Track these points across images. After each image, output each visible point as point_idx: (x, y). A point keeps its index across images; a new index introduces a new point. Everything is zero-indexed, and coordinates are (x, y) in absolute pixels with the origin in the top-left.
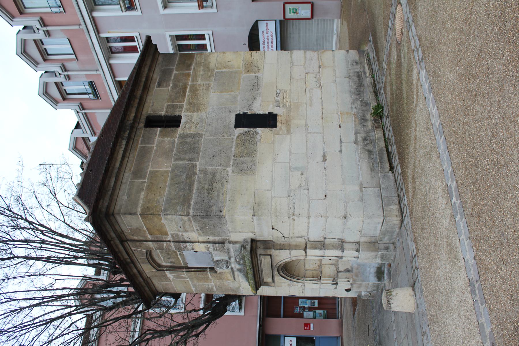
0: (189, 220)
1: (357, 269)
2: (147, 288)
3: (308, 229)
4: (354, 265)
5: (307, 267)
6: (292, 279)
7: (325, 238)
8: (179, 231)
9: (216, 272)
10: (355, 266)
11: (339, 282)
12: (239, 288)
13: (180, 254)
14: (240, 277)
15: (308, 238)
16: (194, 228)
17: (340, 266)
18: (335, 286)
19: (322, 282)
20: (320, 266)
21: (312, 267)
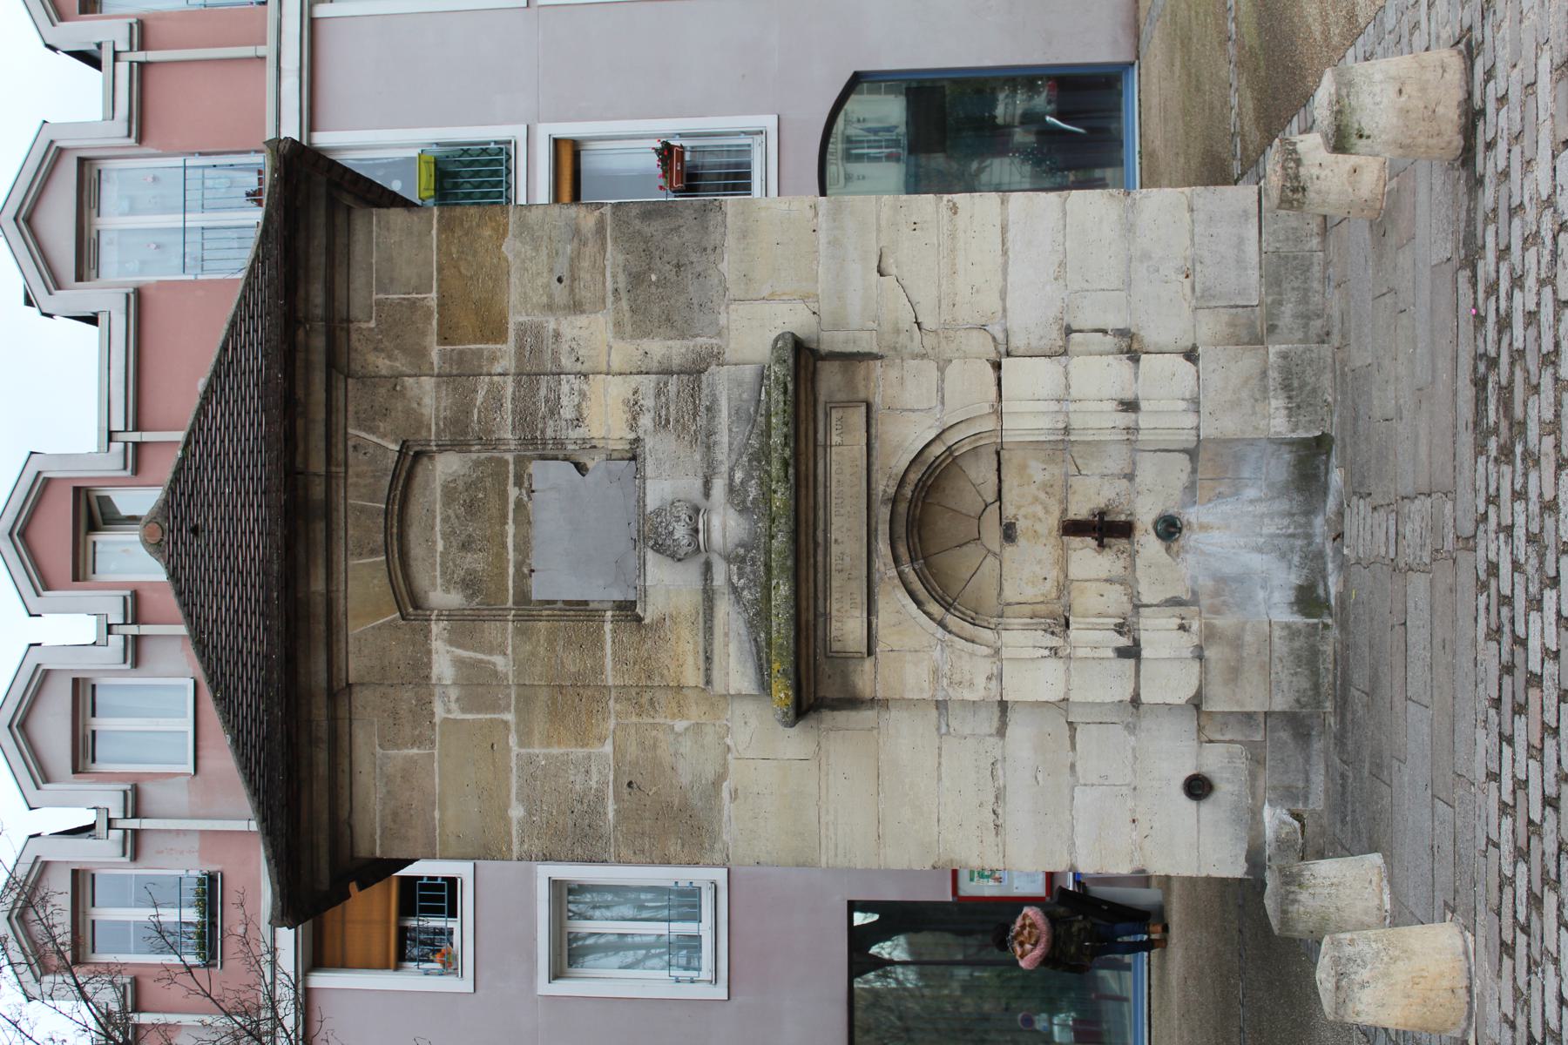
0: (600, 228)
1: (1217, 593)
2: (322, 756)
3: (1005, 280)
4: (1201, 581)
5: (1010, 594)
6: (950, 620)
7: (1069, 331)
8: (550, 307)
9: (639, 619)
10: (1206, 583)
11: (1144, 637)
12: (717, 784)
13: (520, 505)
14: (732, 648)
15: (1006, 332)
16: (609, 285)
17: (1143, 587)
18: (1132, 662)
19: (1073, 633)
20: (1064, 587)
21: (1030, 593)
